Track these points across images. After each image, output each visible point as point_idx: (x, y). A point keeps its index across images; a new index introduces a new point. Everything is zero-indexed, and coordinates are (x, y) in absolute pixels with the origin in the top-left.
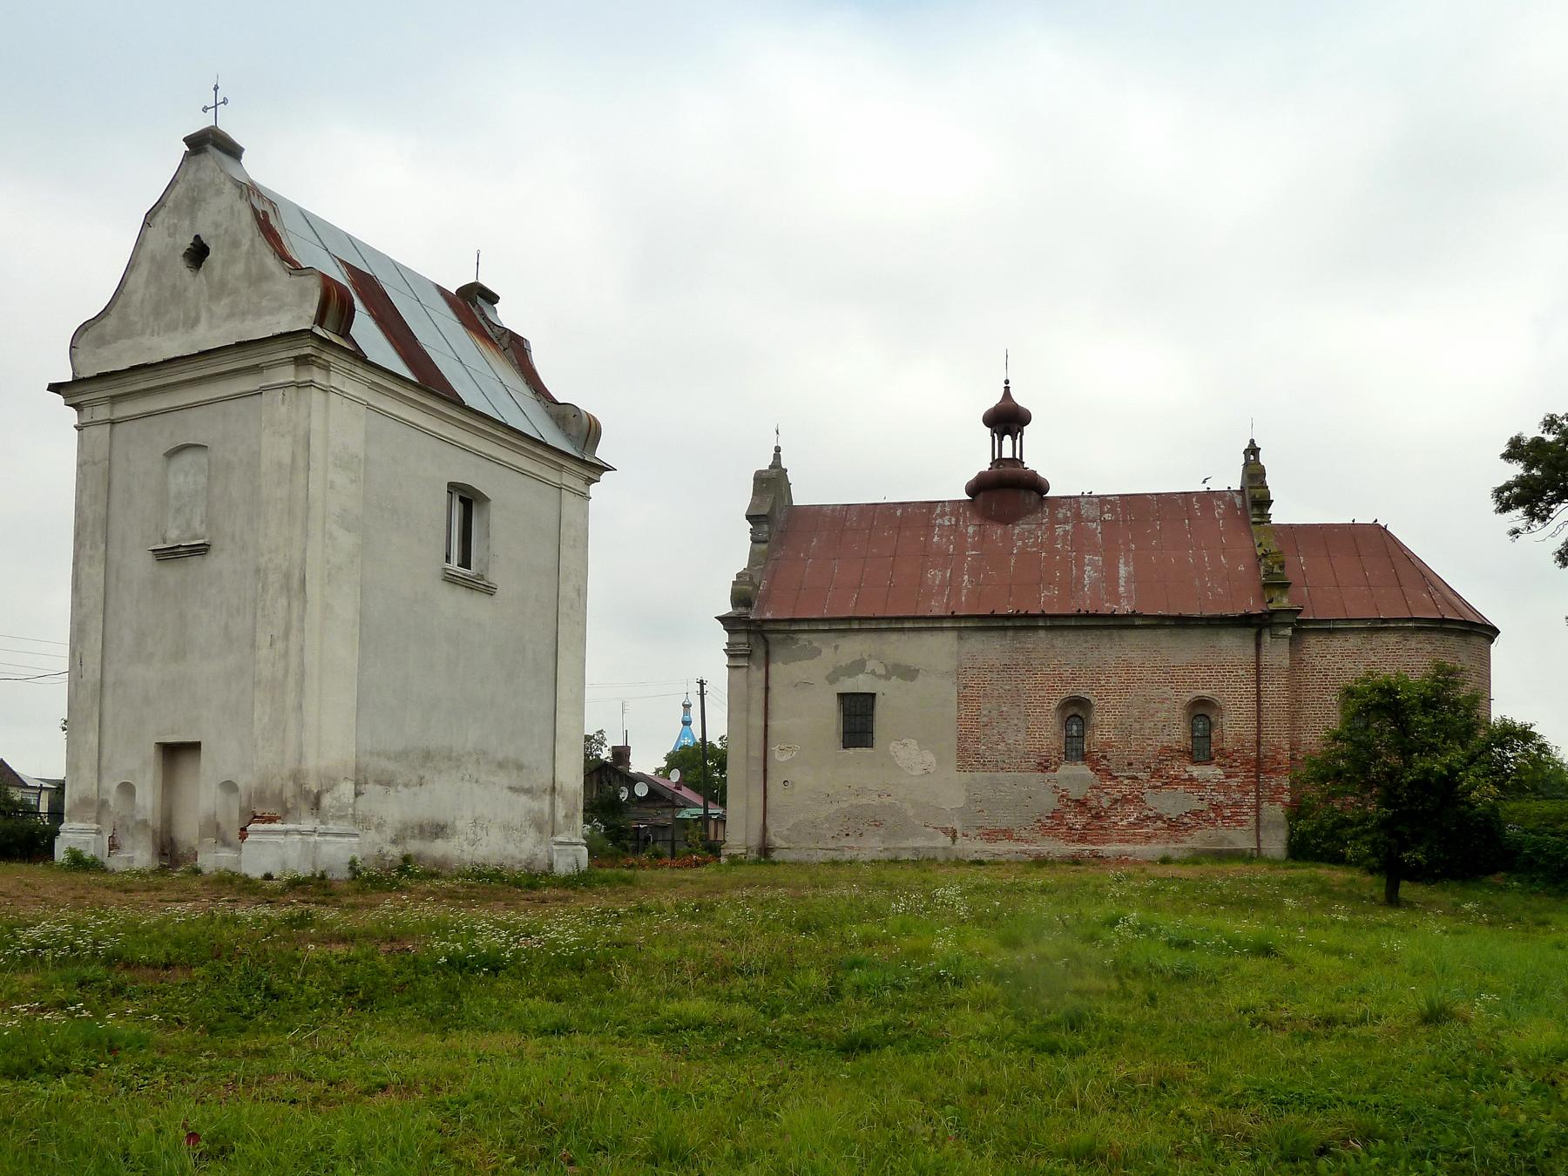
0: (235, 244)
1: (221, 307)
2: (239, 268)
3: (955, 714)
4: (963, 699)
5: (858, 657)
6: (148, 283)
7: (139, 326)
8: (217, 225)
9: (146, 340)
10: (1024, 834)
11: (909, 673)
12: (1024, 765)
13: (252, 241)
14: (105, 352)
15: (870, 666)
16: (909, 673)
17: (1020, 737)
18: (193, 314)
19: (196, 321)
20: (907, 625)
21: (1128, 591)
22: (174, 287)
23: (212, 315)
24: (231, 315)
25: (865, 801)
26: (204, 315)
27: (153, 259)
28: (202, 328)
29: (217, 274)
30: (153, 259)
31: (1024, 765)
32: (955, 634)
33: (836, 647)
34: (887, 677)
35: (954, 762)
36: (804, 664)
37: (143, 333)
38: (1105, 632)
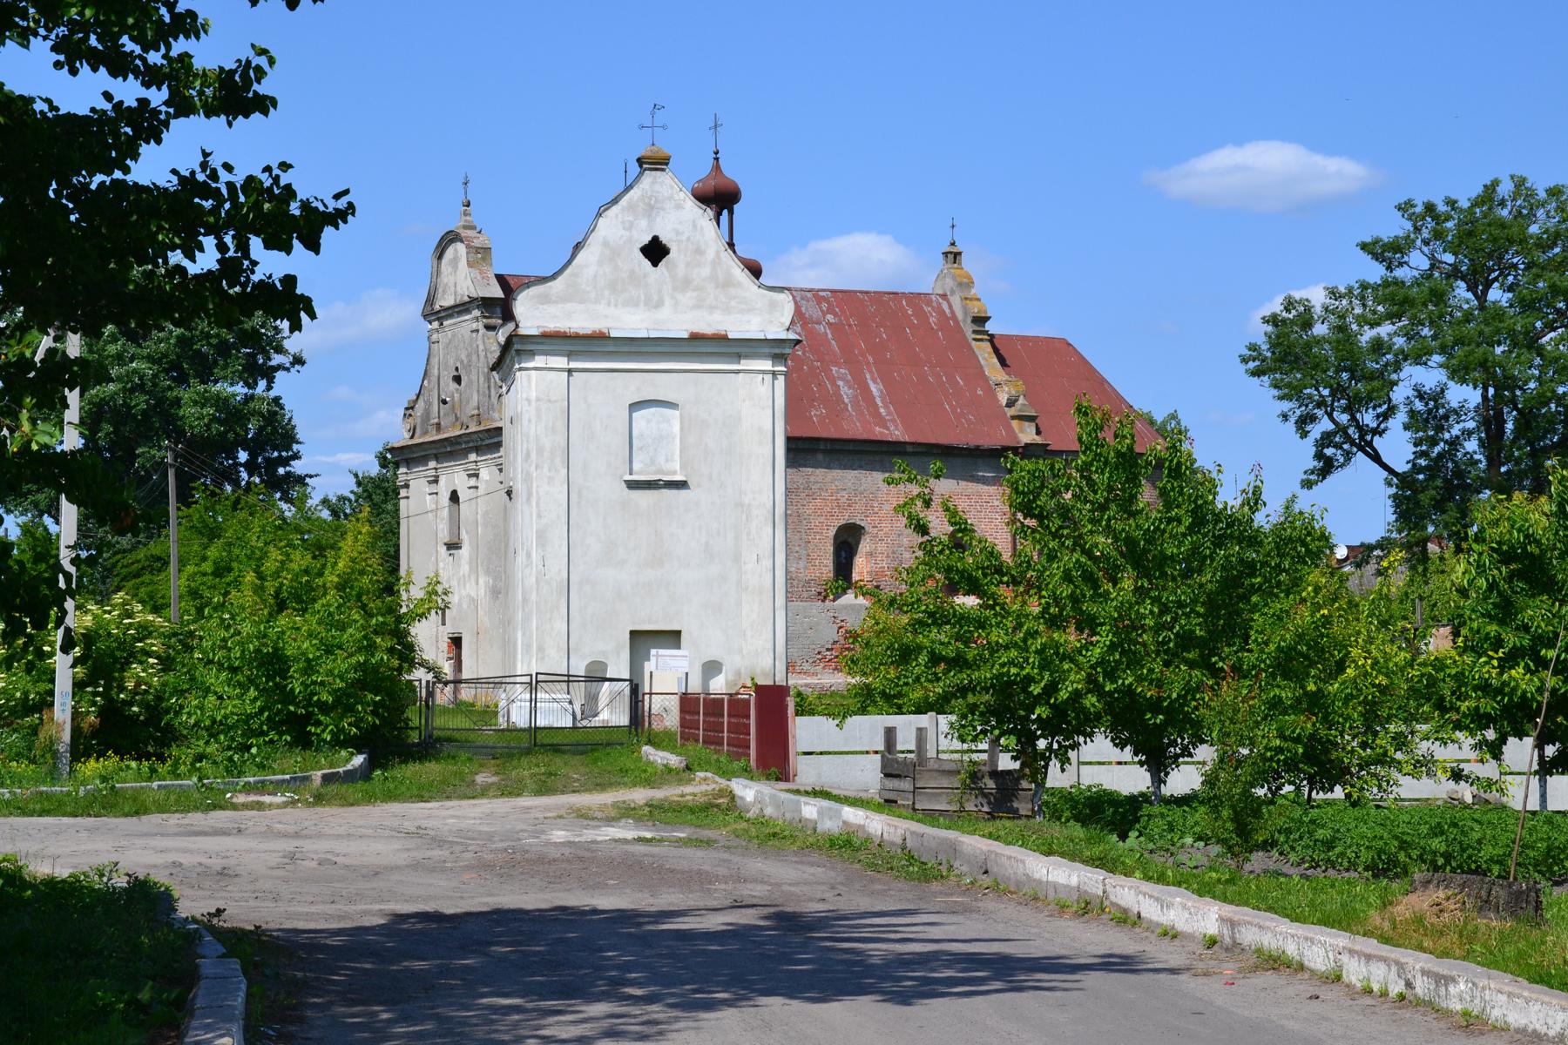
0: (699, 251)
1: (687, 298)
2: (706, 271)
6: (600, 263)
7: (593, 295)
8: (678, 233)
9: (601, 308)
10: (806, 666)
12: (805, 595)
13: (718, 253)
14: (550, 309)
17: (802, 564)
18: (656, 298)
19: (659, 304)
21: (889, 413)
22: (632, 272)
23: (676, 304)
24: (698, 306)
26: (668, 301)
28: (665, 312)
29: (681, 270)
30: (606, 244)
31: (805, 595)
37: (597, 301)
38: (877, 458)
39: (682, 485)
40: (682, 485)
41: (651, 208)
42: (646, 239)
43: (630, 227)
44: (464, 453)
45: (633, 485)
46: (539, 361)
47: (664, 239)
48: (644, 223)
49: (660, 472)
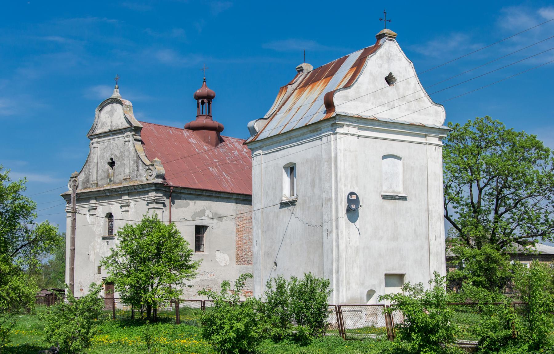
3: (235, 238)
4: (238, 231)
5: (203, 208)
11: (220, 218)
13: (415, 84)
15: (207, 213)
16: (220, 218)
20: (222, 195)
25: (205, 278)
27: (371, 74)
28: (396, 111)
30: (371, 74)
32: (234, 201)
33: (195, 203)
34: (213, 219)
35: (235, 260)
36: (183, 209)
39: (403, 198)
40: (403, 198)
41: (389, 59)
42: (387, 74)
43: (381, 67)
44: (120, 196)
45: (385, 197)
46: (345, 129)
47: (394, 75)
48: (386, 66)
49: (394, 192)
